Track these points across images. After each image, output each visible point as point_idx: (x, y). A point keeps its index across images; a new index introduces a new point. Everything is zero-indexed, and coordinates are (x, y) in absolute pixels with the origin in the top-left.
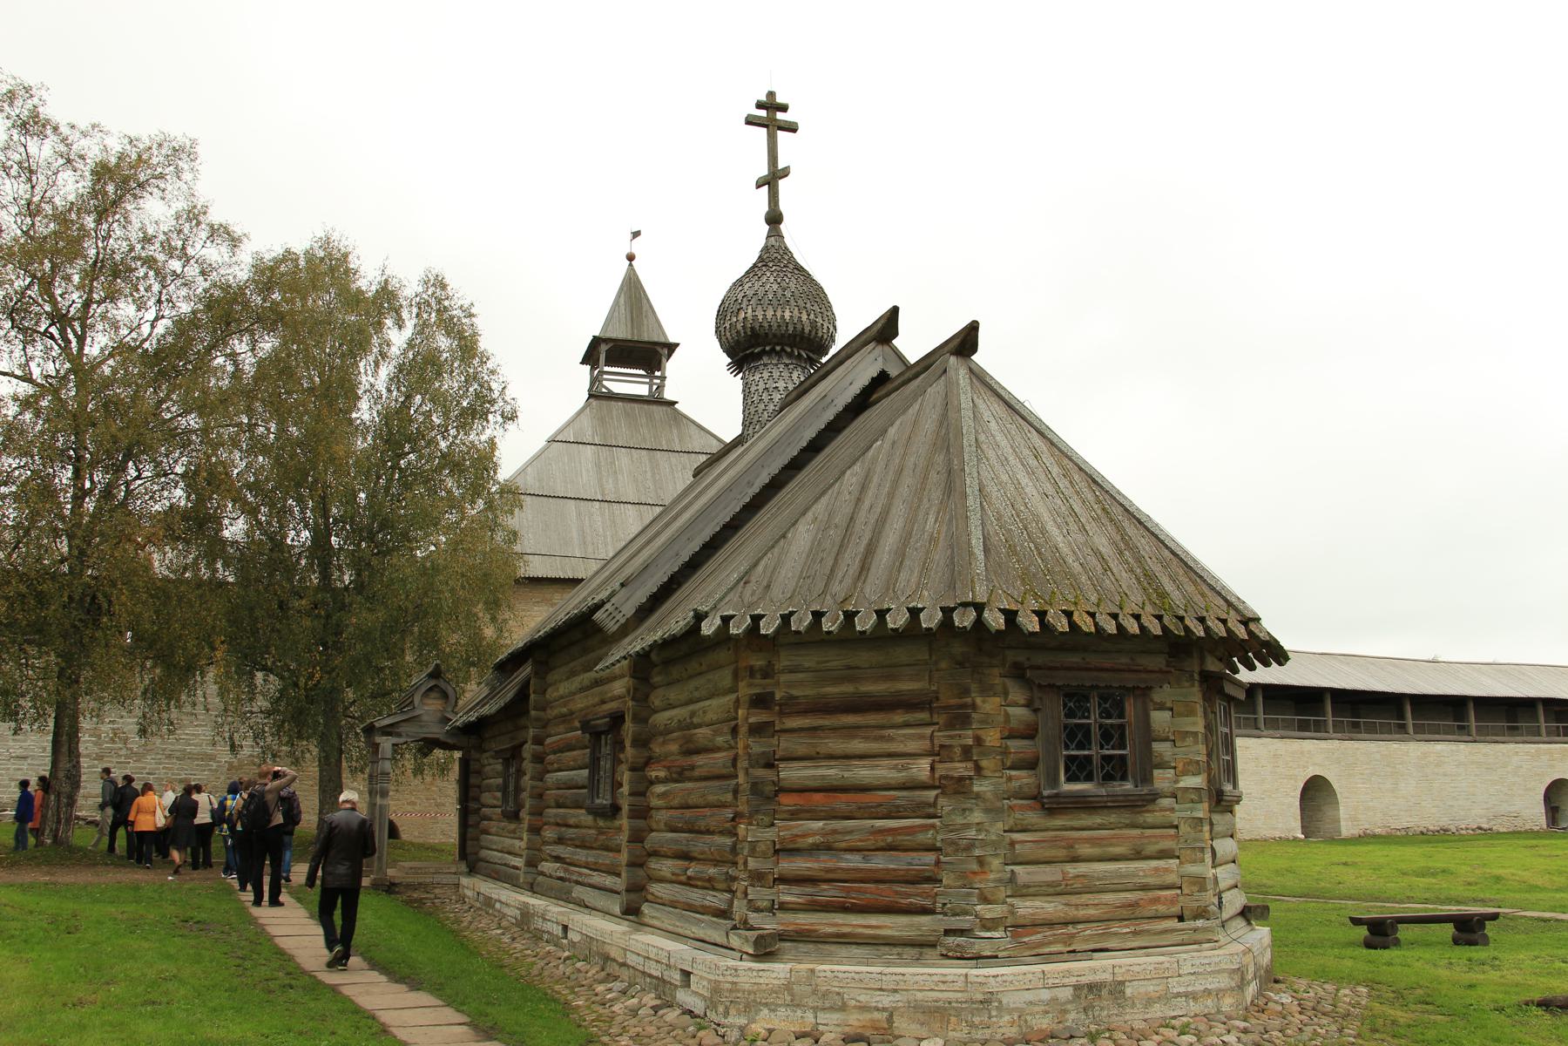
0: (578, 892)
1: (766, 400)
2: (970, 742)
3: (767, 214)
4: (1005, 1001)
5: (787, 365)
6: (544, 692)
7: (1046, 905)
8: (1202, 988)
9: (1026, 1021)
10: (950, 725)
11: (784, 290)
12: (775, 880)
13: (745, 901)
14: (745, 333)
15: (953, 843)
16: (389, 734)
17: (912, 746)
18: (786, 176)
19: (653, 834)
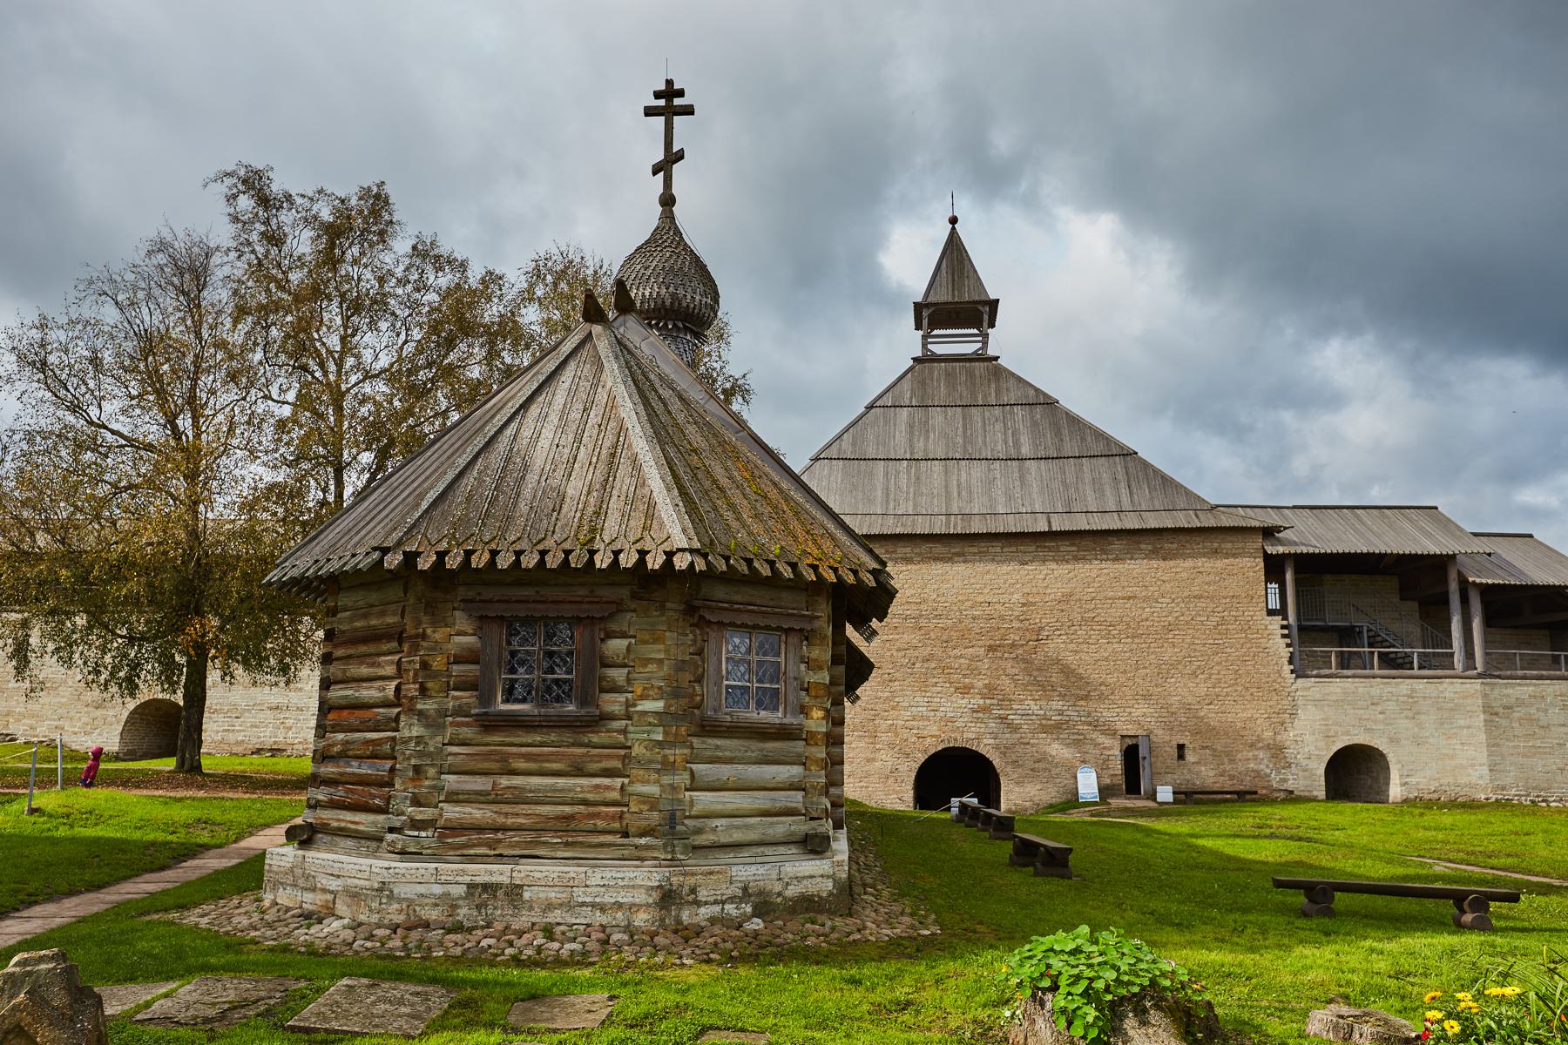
4: (396, 891)
7: (474, 811)
8: (613, 900)
9: (415, 911)
18: (682, 158)
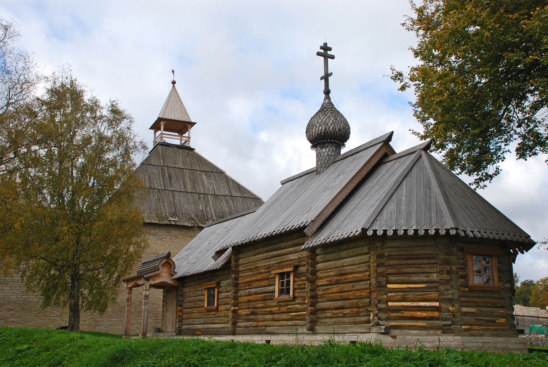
1: (328, 159)
2: (449, 269)
5: (334, 146)
15: (444, 299)
16: (149, 280)
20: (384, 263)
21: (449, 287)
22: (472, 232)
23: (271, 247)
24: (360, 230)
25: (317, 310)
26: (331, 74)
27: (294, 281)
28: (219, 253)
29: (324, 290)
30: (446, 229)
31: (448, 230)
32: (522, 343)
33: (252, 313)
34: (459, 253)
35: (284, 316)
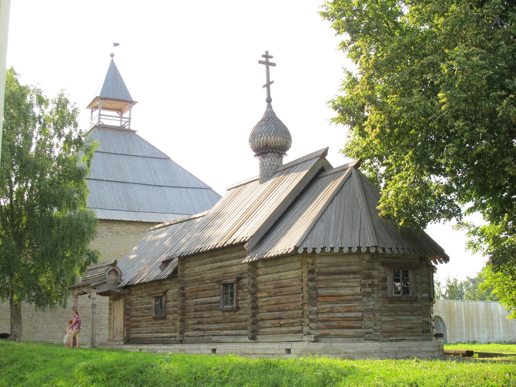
0: (214, 338)
2: (371, 283)
3: (267, 98)
4: (383, 350)
5: (277, 156)
6: (184, 271)
10: (365, 279)
11: (277, 130)
12: (317, 321)
13: (308, 327)
14: (263, 144)
15: (367, 310)
16: (95, 289)
17: (355, 285)
19: (259, 314)
20: (314, 278)
21: (371, 299)
22: (391, 249)
23: (216, 258)
24: (293, 248)
25: (257, 321)
26: (272, 82)
27: (238, 293)
28: (166, 263)
29: (264, 302)
30: (367, 247)
31: (368, 248)
32: (434, 346)
33: (199, 323)
34: (381, 268)
35: (229, 325)
